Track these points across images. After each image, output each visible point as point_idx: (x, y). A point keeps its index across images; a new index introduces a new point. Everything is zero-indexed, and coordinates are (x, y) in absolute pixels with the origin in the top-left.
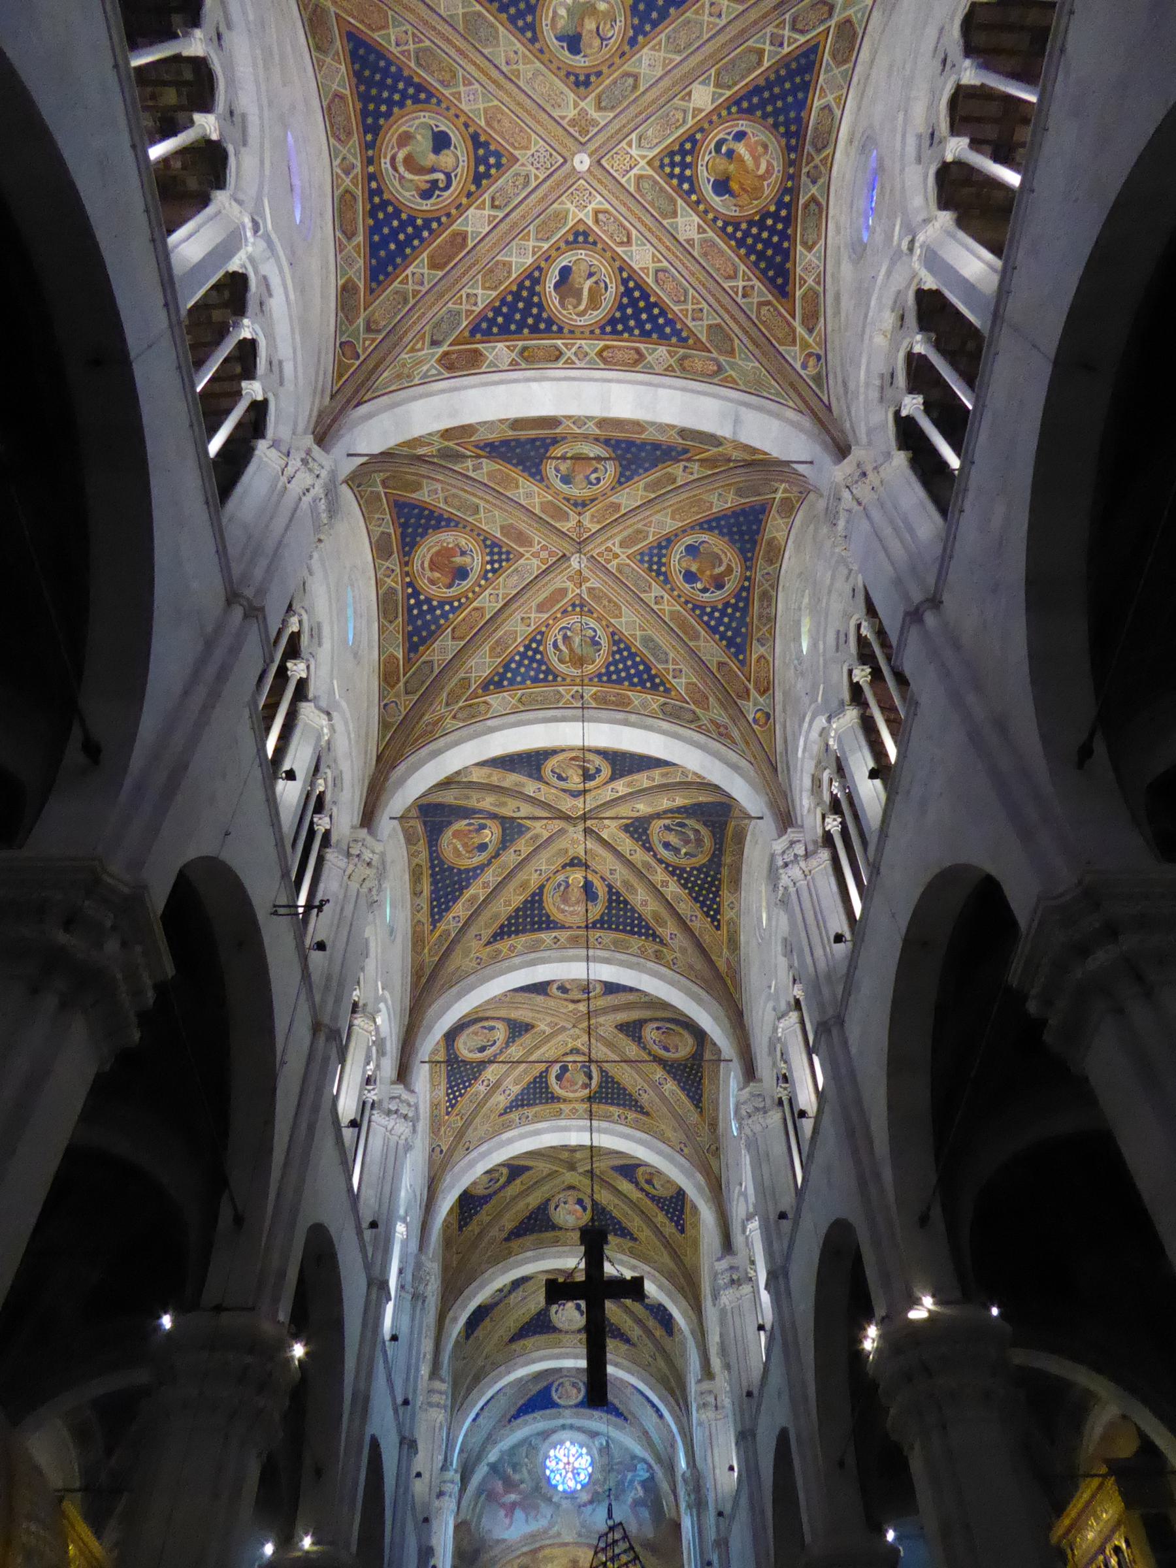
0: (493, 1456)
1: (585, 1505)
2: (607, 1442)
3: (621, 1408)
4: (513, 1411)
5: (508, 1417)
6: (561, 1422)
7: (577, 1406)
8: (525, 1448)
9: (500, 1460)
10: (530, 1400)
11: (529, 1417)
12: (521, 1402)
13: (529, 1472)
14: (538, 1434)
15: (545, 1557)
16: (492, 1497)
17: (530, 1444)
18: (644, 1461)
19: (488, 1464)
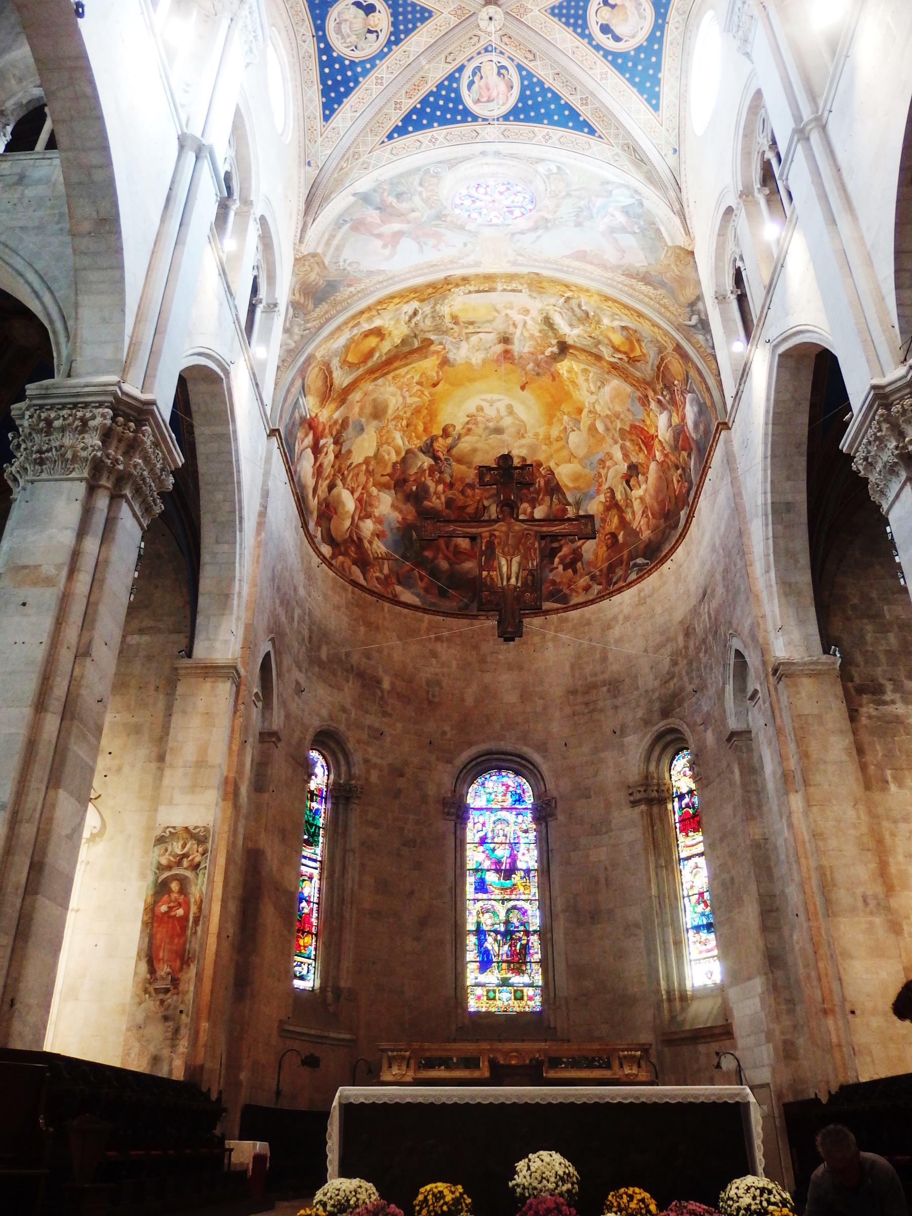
0: (364, 184)
1: (522, 233)
2: (558, 168)
3: (586, 113)
4: (396, 119)
5: (389, 126)
6: (480, 147)
7: (506, 117)
8: (417, 178)
9: (375, 190)
10: (424, 101)
11: (424, 136)
12: (409, 104)
13: (426, 201)
14: (440, 162)
15: (455, 320)
16: (359, 226)
17: (427, 172)
18: (627, 187)
19: (354, 195)
